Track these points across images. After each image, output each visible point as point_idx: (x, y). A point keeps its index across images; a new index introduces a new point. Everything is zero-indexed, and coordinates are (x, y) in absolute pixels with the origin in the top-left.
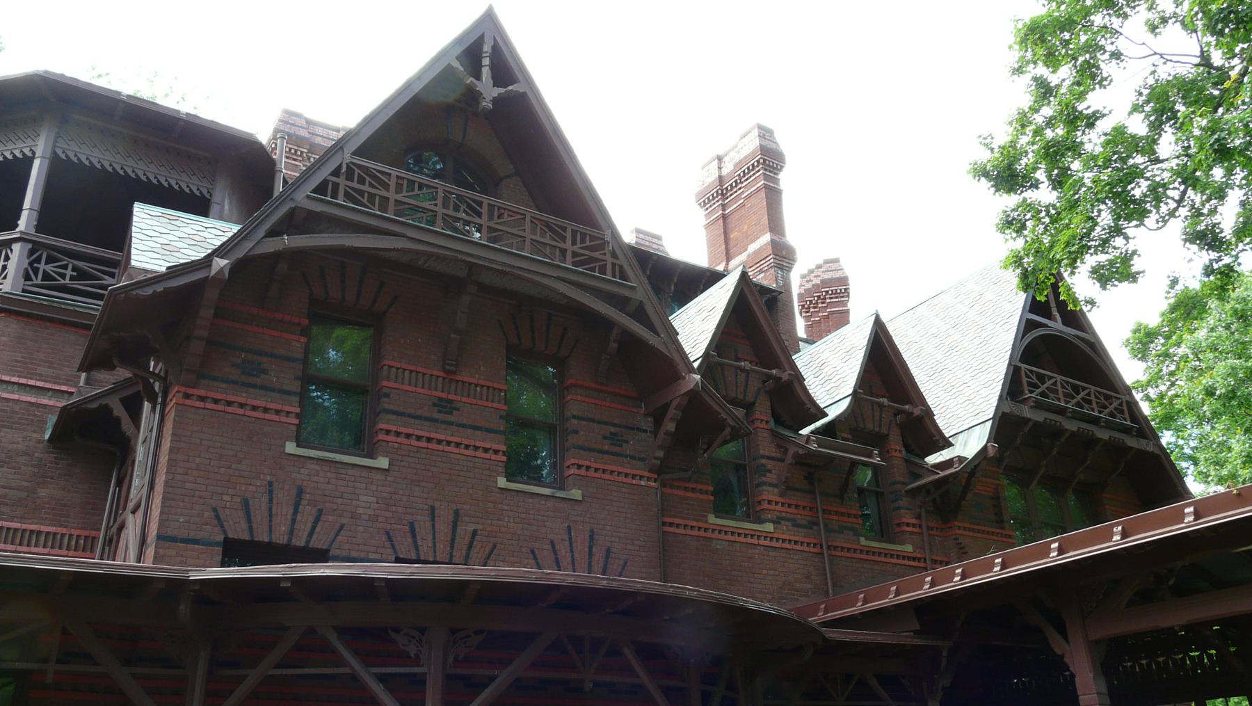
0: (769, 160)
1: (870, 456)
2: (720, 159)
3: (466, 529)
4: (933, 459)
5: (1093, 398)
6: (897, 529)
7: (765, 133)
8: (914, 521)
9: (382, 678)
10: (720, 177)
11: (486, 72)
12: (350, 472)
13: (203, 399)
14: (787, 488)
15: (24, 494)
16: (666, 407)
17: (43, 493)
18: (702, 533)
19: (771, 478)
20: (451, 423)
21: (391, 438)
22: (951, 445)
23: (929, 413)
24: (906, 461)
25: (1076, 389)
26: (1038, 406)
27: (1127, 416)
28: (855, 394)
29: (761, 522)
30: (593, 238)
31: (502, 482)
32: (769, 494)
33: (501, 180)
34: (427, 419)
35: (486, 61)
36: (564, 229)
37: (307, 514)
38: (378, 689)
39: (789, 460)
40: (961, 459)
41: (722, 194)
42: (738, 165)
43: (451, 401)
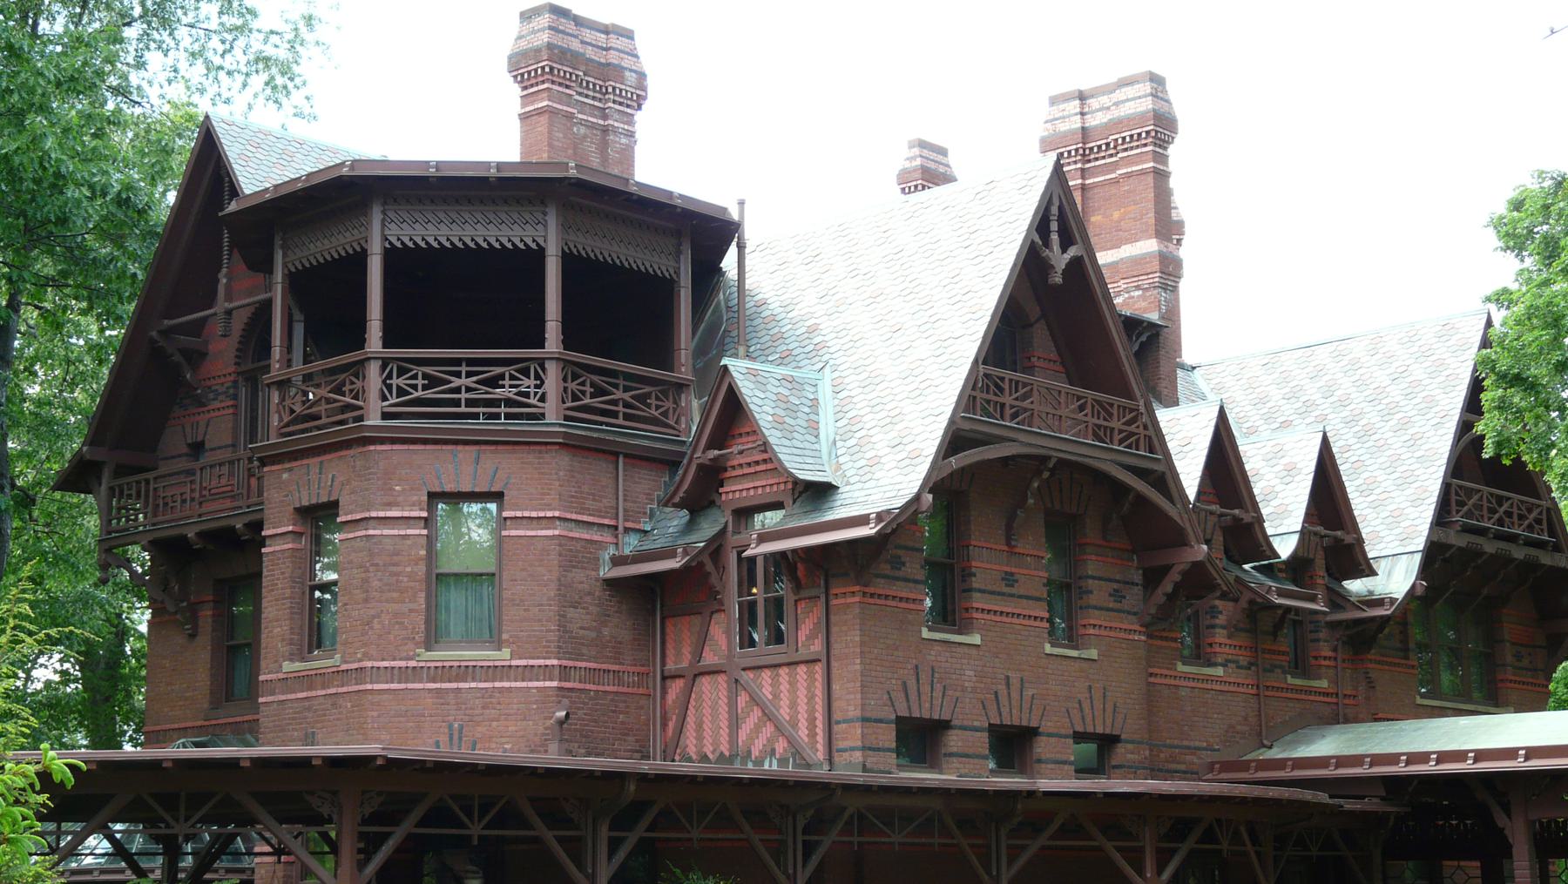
0: (1161, 128)
1: (1313, 599)
2: (1082, 97)
3: (1028, 693)
4: (1355, 586)
5: (1515, 510)
6: (1313, 661)
7: (1157, 80)
8: (1330, 654)
9: (1119, 849)
10: (1083, 128)
11: (1055, 237)
12: (959, 649)
13: (872, 595)
14: (1233, 629)
15: (594, 635)
16: (1167, 569)
17: (606, 631)
18: (1172, 682)
19: (1221, 620)
20: (1012, 595)
21: (979, 615)
22: (1373, 573)
23: (1360, 541)
24: (1328, 588)
25: (1500, 500)
26: (1468, 530)
27: (1545, 526)
28: (1303, 533)
29: (1211, 664)
30: (1131, 410)
31: (1048, 649)
32: (1220, 636)
33: (1031, 325)
34: (999, 594)
35: (1054, 226)
36: (1112, 405)
37: (938, 687)
38: (1118, 857)
39: (1243, 603)
40: (1393, 601)
41: (1084, 155)
42: (1116, 125)
43: (1012, 574)
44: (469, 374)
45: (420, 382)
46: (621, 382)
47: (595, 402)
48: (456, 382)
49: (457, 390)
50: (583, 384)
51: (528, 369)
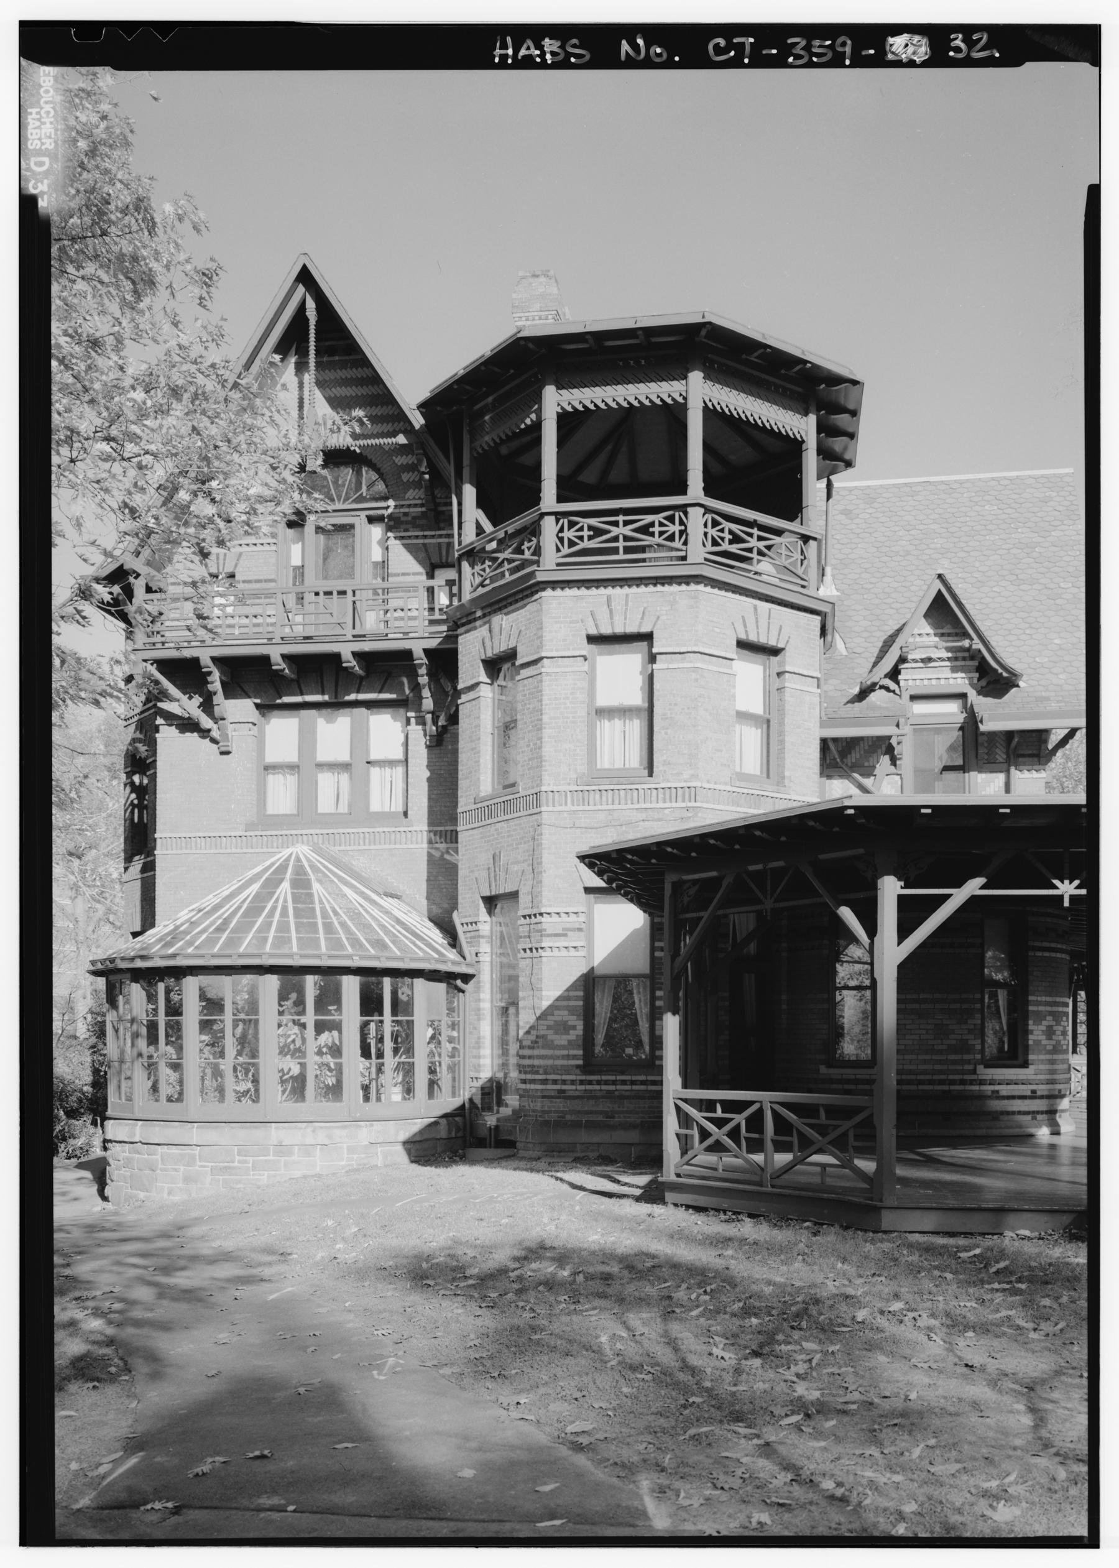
44: (626, 523)
45: (586, 533)
46: (755, 531)
47: (734, 548)
48: (615, 531)
49: (616, 539)
50: (722, 530)
51: (674, 515)
